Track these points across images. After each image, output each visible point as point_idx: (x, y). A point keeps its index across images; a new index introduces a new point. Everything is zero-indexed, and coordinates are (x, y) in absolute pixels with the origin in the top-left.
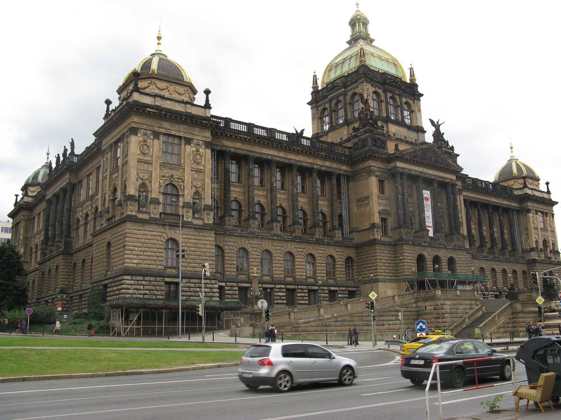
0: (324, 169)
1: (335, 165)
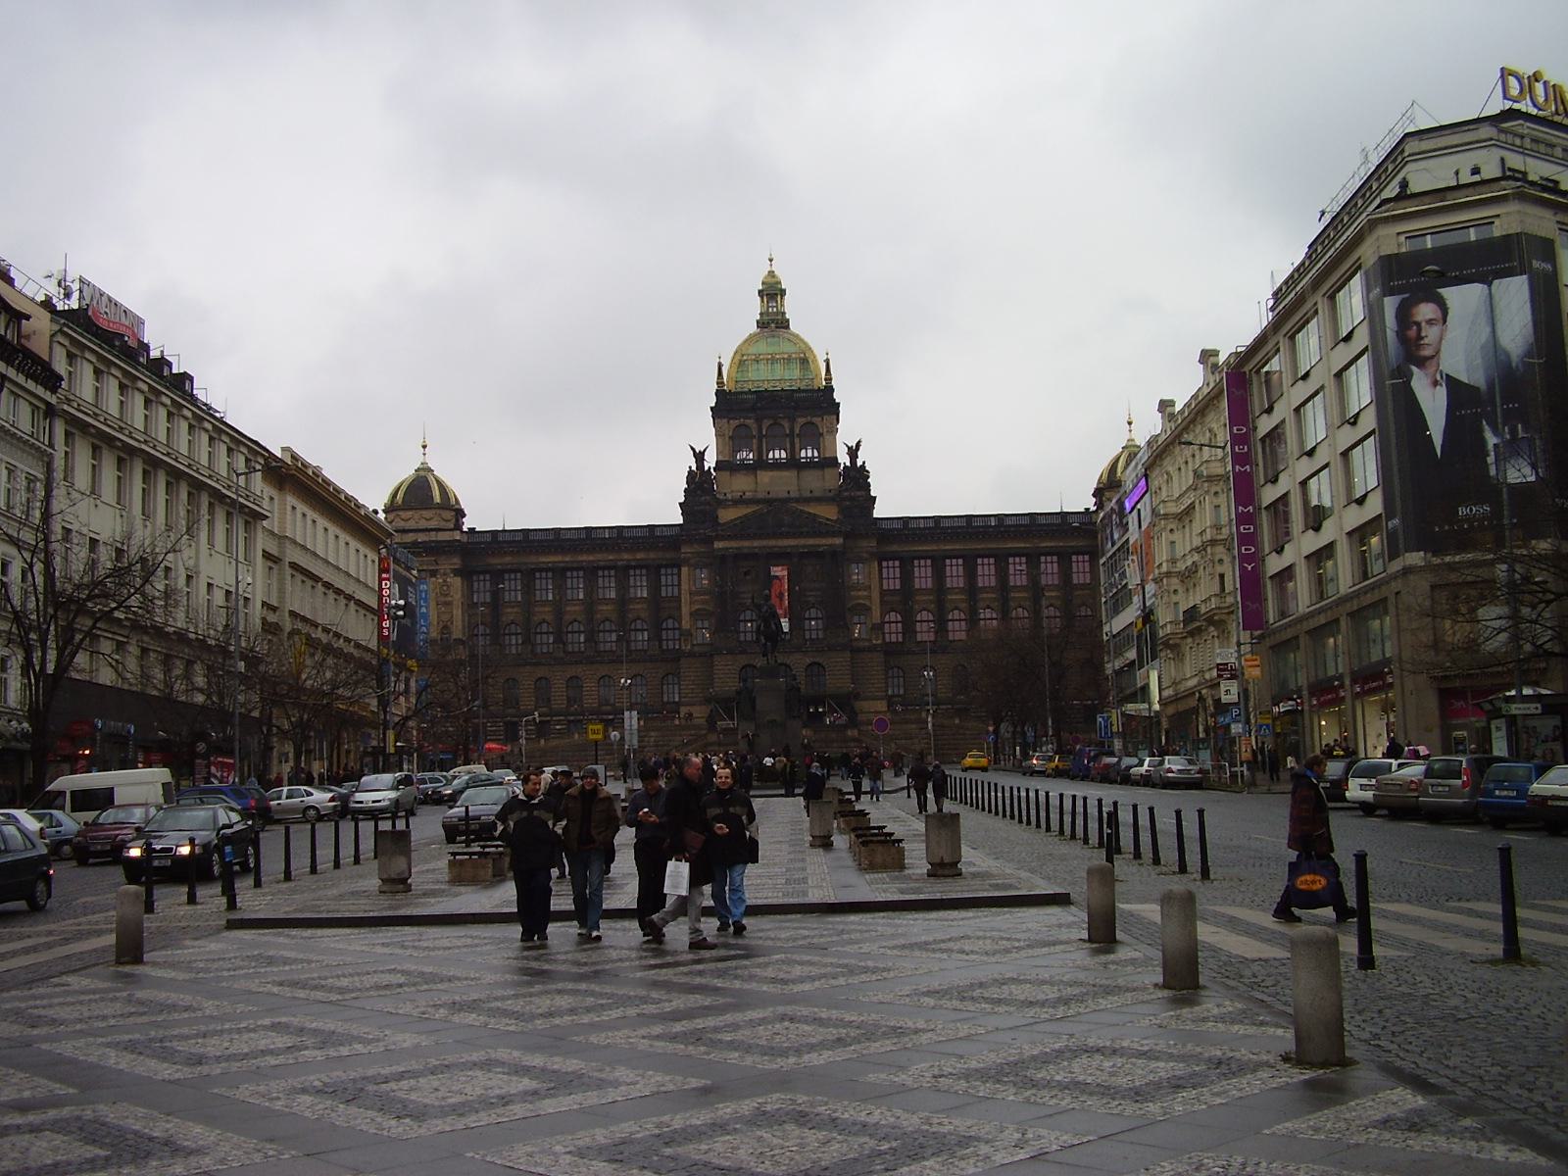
0: (633, 564)
1: (652, 555)
